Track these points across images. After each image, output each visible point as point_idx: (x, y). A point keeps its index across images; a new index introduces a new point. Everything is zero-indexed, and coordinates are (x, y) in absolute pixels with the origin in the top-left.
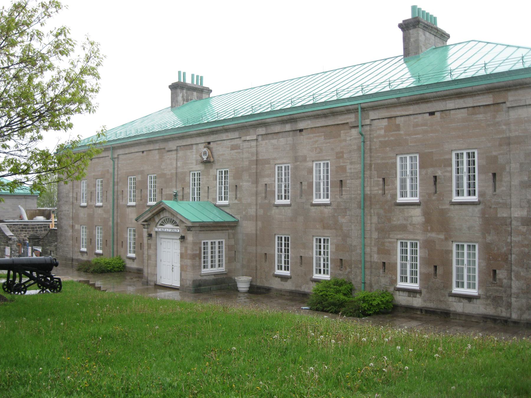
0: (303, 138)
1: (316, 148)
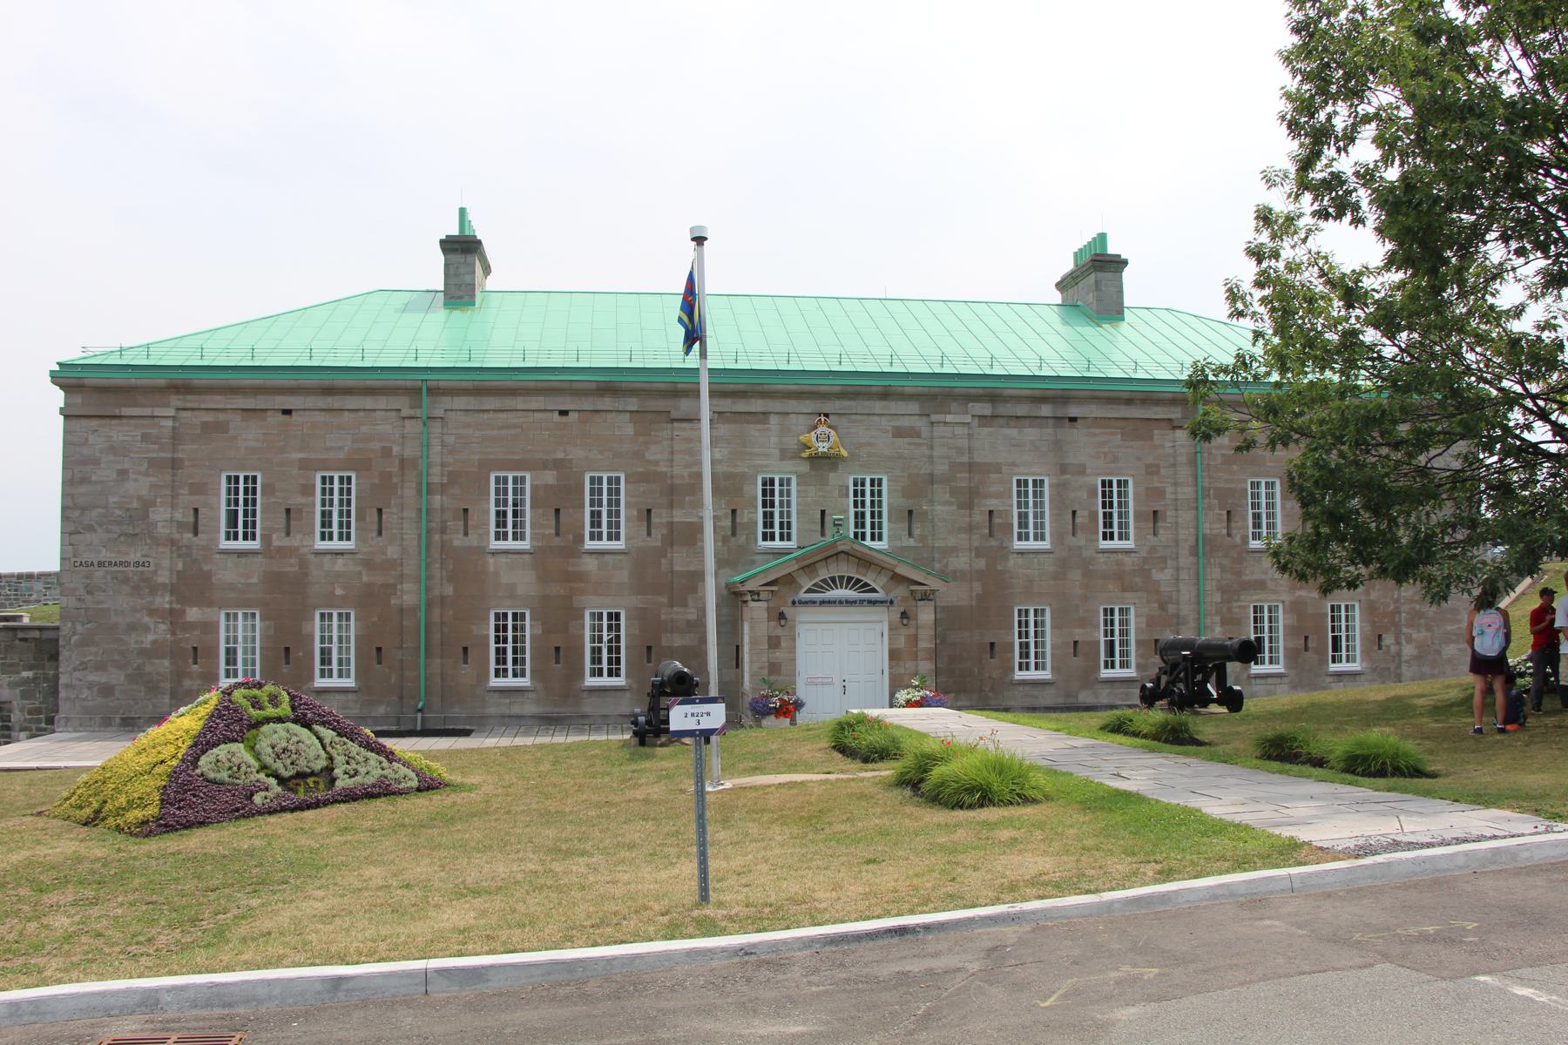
0: (1076, 434)
1: (1105, 454)
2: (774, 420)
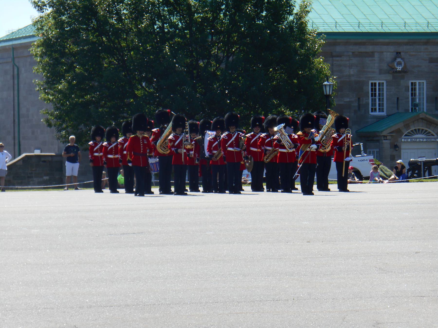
2: (377, 55)
